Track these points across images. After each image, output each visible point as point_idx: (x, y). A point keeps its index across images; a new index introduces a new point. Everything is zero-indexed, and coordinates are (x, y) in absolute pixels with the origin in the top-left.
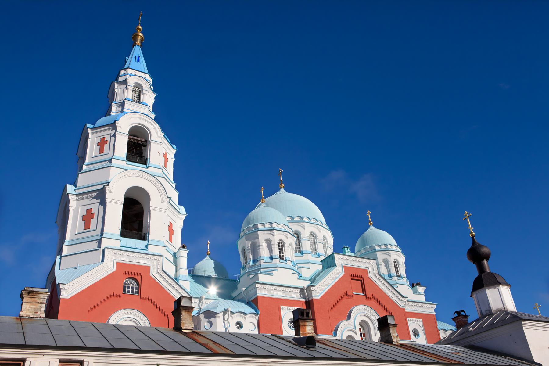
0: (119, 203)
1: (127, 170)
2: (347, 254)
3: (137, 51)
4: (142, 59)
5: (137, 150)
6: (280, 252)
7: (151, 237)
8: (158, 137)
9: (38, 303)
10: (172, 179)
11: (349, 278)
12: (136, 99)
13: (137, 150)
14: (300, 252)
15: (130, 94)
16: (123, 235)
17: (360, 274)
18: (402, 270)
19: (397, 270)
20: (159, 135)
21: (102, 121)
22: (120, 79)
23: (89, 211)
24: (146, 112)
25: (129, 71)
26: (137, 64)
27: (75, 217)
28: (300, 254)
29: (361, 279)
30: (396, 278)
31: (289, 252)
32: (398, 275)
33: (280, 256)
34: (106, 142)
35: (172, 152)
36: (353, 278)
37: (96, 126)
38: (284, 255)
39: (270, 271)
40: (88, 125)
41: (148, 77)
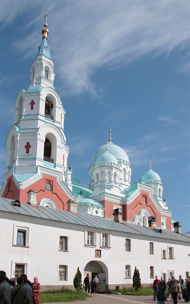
0: (43, 142)
8: (59, 104)
9: (75, 207)
15: (43, 73)
17: (145, 194)
19: (159, 194)
20: (60, 103)
34: (34, 103)
35: (64, 113)
39: (110, 187)
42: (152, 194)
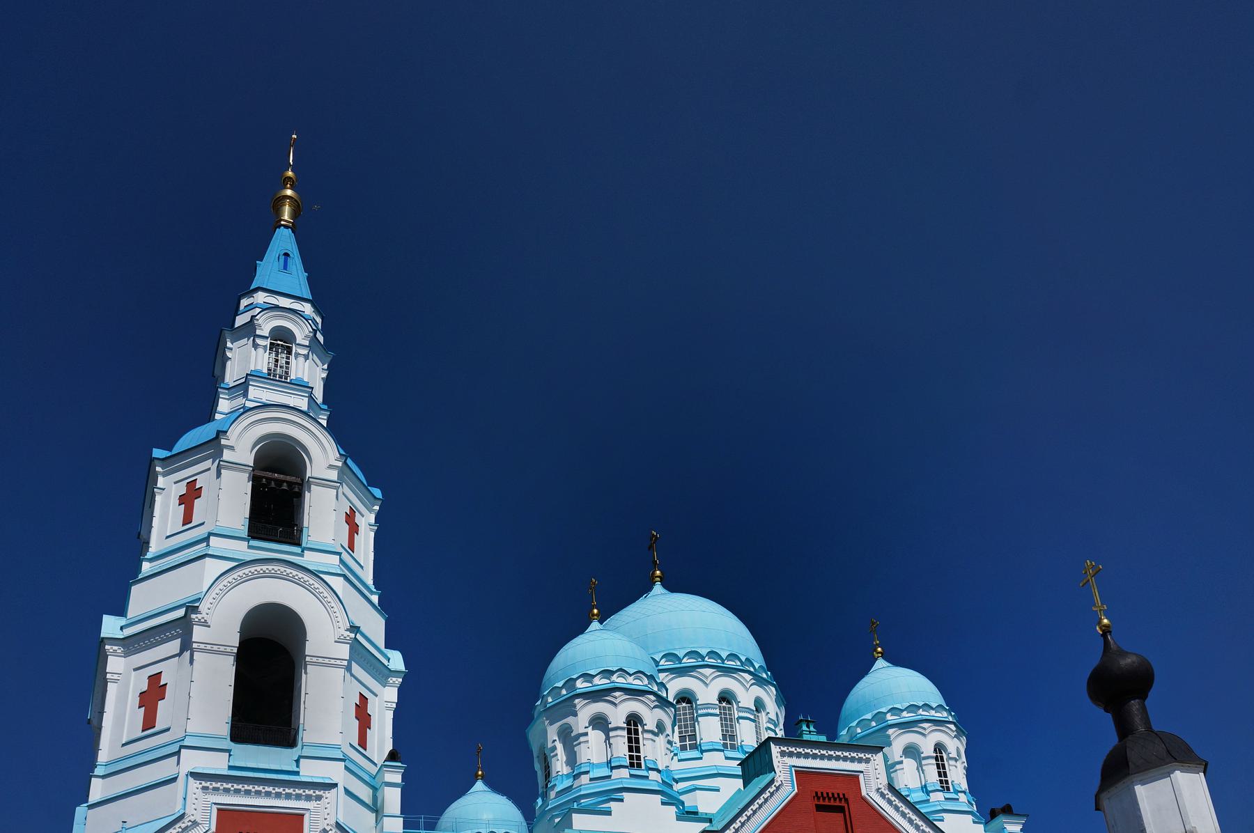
1: (244, 564)
2: (806, 737)
3: (284, 240)
4: (296, 262)
5: (276, 508)
6: (630, 749)
7: (308, 735)
8: (331, 467)
10: (370, 581)
11: (810, 804)
12: (275, 372)
13: (276, 508)
14: (694, 747)
16: (238, 735)
17: (838, 789)
18: (957, 774)
19: (942, 773)
21: (188, 440)
22: (240, 321)
23: (155, 679)
24: (303, 404)
25: (261, 298)
26: (283, 276)
27: (122, 699)
28: (695, 754)
29: (843, 804)
30: (940, 796)
31: (654, 750)
32: (945, 785)
33: (631, 757)
36: (821, 802)
37: (175, 451)
38: (642, 755)
40: (158, 453)
41: (307, 309)
42: (883, 781)
